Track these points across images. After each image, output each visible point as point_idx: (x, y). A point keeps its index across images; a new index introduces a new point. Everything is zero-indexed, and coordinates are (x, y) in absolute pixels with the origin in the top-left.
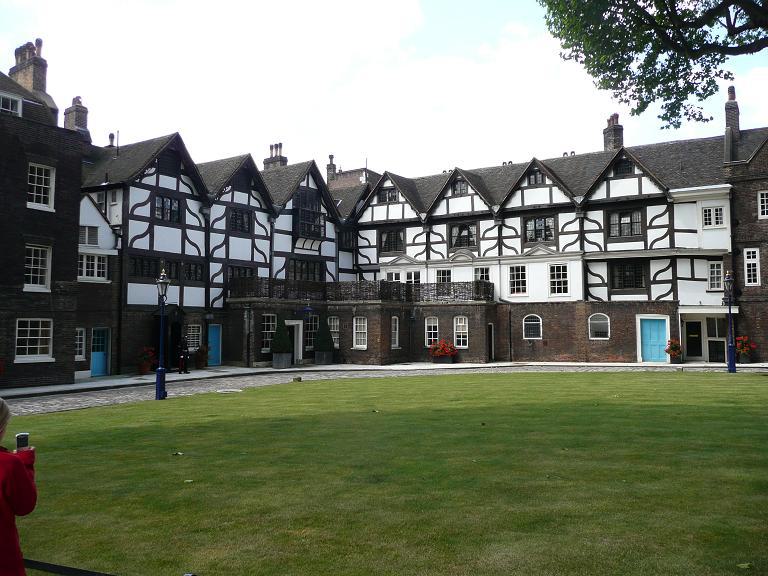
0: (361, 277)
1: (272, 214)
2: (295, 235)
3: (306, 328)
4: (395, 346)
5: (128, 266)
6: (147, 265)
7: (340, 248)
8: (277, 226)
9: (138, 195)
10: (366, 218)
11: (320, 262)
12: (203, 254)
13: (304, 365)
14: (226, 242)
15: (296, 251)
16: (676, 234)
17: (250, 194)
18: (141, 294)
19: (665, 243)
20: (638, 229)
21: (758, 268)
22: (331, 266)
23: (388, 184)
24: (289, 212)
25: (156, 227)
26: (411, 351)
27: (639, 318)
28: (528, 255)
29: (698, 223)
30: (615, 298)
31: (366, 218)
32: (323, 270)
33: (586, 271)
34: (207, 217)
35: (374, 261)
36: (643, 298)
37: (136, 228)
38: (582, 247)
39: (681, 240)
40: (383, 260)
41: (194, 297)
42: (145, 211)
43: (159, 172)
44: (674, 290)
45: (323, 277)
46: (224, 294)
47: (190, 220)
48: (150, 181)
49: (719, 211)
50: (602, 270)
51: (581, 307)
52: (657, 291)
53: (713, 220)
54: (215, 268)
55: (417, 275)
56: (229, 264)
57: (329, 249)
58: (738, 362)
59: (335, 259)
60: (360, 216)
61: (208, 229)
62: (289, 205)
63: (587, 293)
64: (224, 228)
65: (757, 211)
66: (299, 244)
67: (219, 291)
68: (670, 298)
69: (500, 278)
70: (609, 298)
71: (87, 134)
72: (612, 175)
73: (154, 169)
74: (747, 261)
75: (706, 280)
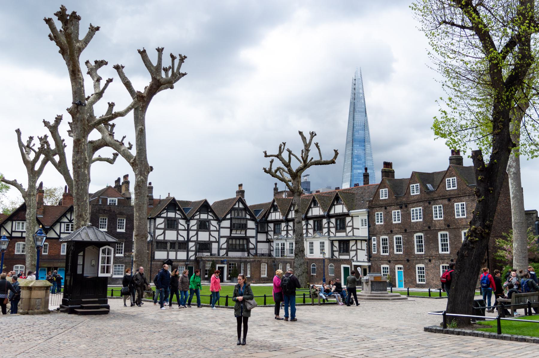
0: (271, 245)
1: (219, 221)
2: (232, 228)
3: (229, 267)
4: (249, 276)
5: (155, 244)
6: (162, 245)
7: (258, 232)
8: (221, 226)
9: (159, 221)
10: (269, 219)
11: (247, 239)
12: (186, 239)
13: (227, 283)
14: (197, 234)
15: (232, 235)
16: (354, 230)
17: (208, 214)
18: (160, 255)
19: (351, 234)
21: (376, 246)
22: (253, 241)
24: (228, 219)
25: (166, 231)
27: (342, 266)
28: (314, 237)
29: (359, 225)
31: (269, 219)
32: (248, 242)
34: (188, 225)
35: (272, 238)
36: (347, 257)
37: (158, 232)
38: (329, 234)
39: (357, 233)
40: (275, 237)
42: (162, 226)
43: (167, 212)
44: (356, 254)
45: (248, 245)
46: (196, 254)
47: (180, 227)
48: (164, 215)
50: (336, 244)
53: (364, 225)
54: (191, 244)
55: (284, 245)
56: (197, 242)
57: (251, 233)
58: (357, 285)
59: (256, 237)
60: (267, 217)
61: (188, 230)
62: (229, 216)
63: (333, 255)
64: (196, 229)
65: (375, 221)
66: (234, 232)
67: (193, 253)
71: (152, 196)
72: (335, 203)
73: (165, 211)
74: (373, 243)
75: (364, 250)
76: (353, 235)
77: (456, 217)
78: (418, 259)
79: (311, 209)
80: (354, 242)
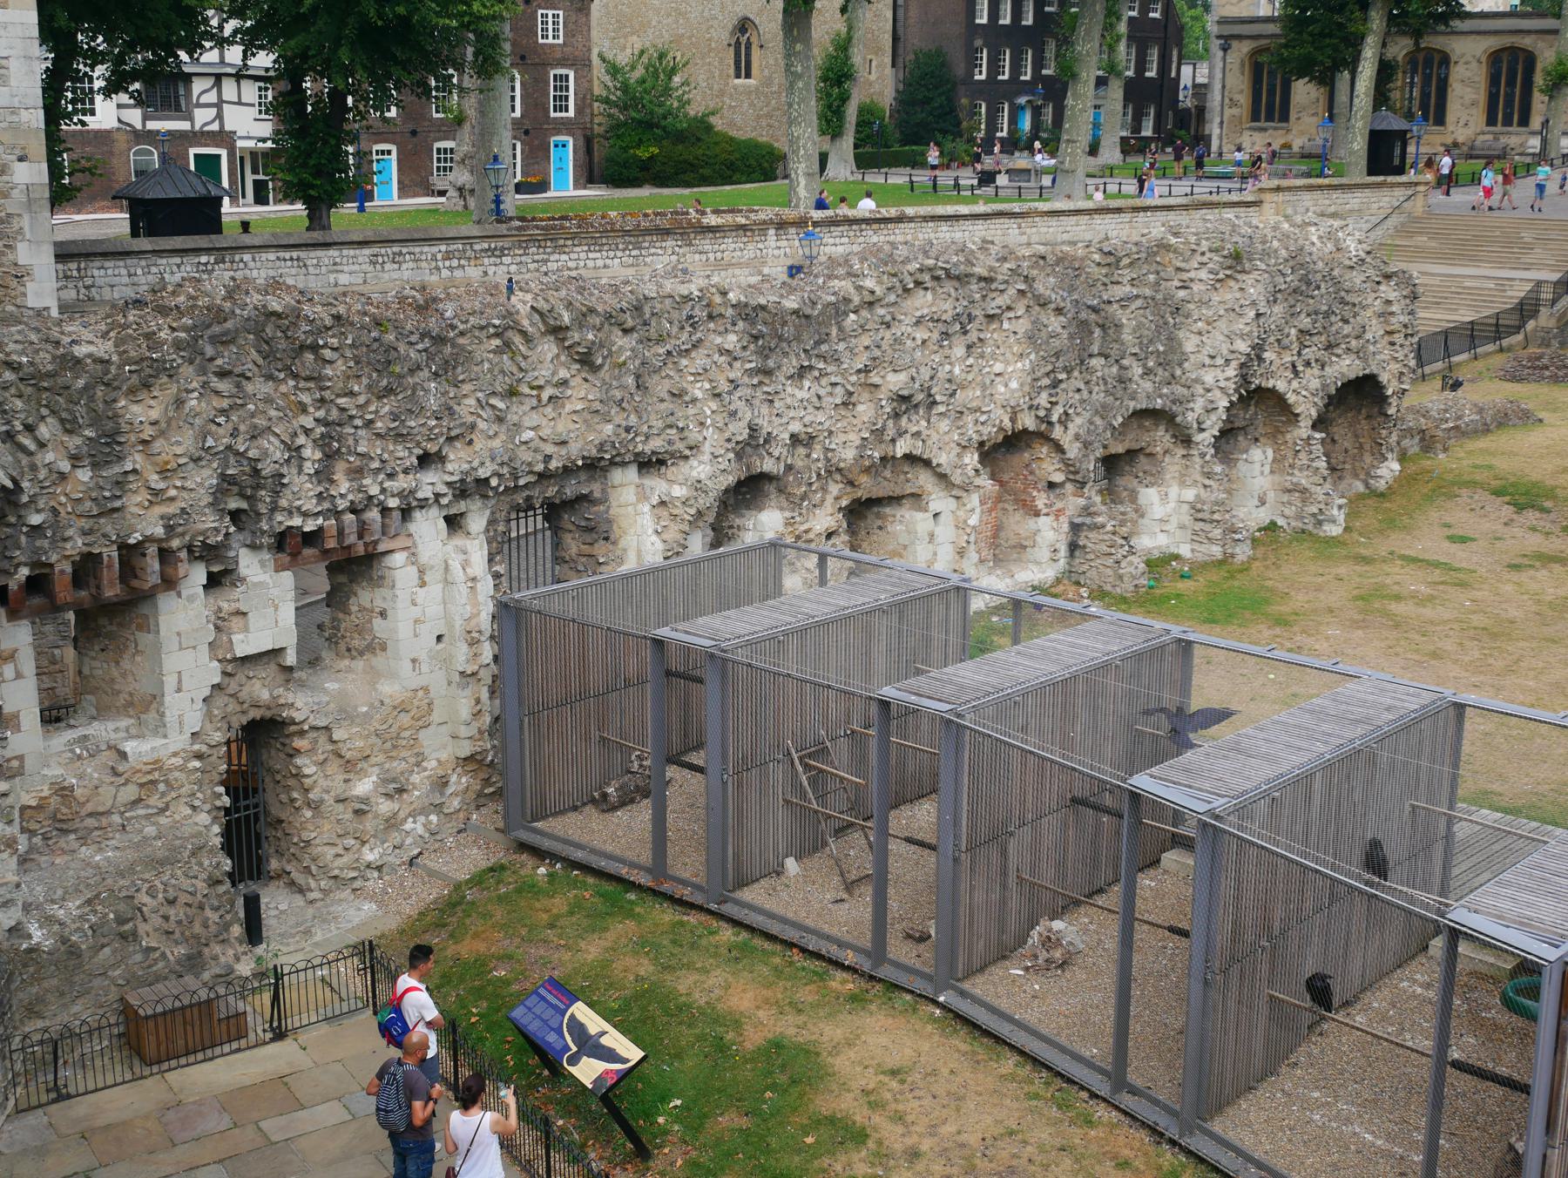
27: (192, 151)
30: (152, 125)
36: (184, 126)
44: (219, 116)
51: (122, 139)
52: (202, 116)
68: (215, 127)
70: (144, 125)
75: (253, 105)
76: (222, 61)
77: (540, 41)
78: (444, 128)
80: (210, 82)
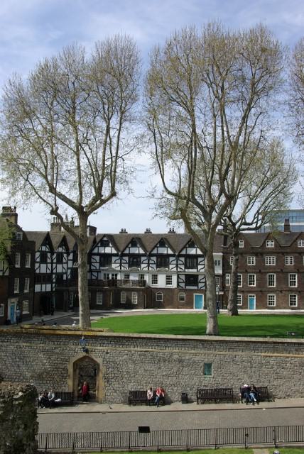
0: (92, 274)
10: (96, 251)
20: (195, 265)
23: (105, 239)
26: (118, 305)
27: (194, 294)
31: (96, 251)
33: (178, 278)
35: (98, 268)
40: (101, 268)
41: (48, 288)
49: (219, 261)
50: (183, 277)
61: (52, 263)
63: (178, 285)
68: (204, 288)
69: (147, 278)
79: (156, 249)
